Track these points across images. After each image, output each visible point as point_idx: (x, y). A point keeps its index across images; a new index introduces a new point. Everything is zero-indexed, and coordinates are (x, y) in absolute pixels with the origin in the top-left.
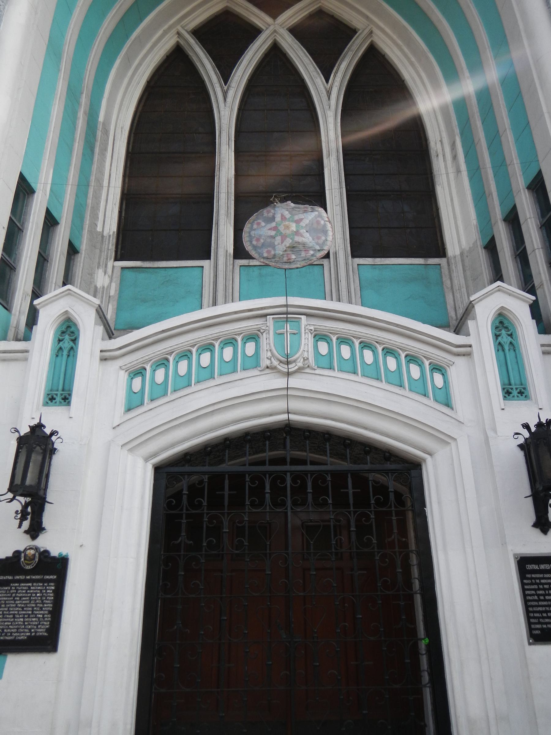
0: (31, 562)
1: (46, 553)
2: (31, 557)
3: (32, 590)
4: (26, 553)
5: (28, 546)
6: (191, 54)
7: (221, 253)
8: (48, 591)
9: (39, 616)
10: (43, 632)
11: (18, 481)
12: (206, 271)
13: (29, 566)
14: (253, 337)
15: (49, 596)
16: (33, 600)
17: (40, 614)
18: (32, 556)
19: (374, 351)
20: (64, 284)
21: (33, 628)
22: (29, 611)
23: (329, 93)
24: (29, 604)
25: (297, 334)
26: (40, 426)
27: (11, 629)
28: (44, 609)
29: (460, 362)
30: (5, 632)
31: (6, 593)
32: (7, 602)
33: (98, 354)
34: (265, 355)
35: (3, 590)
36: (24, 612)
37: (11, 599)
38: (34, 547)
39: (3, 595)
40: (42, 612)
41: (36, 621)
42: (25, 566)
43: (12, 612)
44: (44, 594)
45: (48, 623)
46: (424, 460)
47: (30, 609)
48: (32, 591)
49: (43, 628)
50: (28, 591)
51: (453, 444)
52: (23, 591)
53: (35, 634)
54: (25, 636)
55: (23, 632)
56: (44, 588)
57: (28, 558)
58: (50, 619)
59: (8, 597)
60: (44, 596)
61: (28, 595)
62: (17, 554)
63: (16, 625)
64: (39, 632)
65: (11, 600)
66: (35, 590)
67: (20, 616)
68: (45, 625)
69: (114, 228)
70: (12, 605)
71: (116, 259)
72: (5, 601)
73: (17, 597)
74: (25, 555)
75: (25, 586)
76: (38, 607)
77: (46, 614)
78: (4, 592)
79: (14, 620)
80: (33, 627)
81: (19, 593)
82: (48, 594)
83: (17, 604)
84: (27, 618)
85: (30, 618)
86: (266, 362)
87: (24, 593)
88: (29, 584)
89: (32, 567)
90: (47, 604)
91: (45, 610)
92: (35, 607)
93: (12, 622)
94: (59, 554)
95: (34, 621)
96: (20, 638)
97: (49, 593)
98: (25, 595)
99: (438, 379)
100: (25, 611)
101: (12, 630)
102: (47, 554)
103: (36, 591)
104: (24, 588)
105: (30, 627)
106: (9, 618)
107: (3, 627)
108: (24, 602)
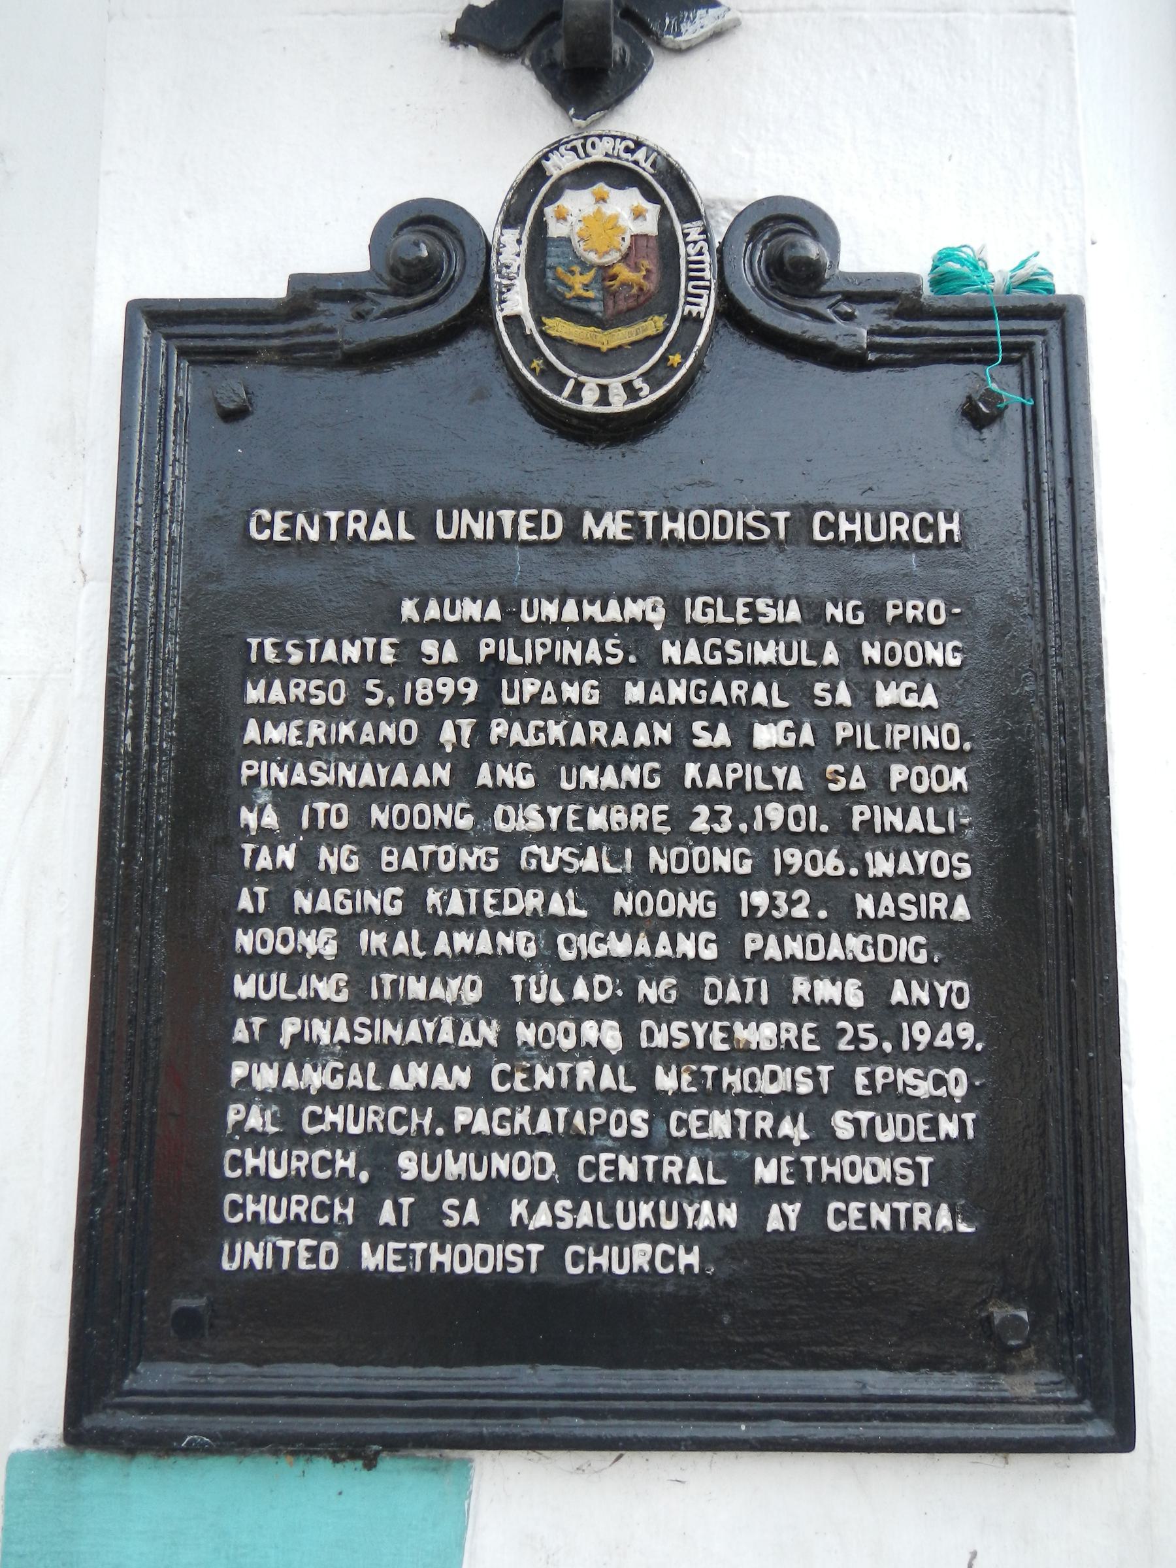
0: (622, 336)
2: (626, 273)
3: (692, 670)
4: (540, 225)
5: (555, 147)
8: (886, 696)
9: (826, 991)
10: (903, 1193)
13: (616, 385)
15: (912, 753)
16: (712, 796)
17: (840, 970)
18: (625, 258)
21: (775, 1145)
22: (690, 924)
24: (664, 842)
27: (484, 1145)
28: (865, 904)
30: (416, 1186)
31: (356, 708)
32: (379, 816)
35: (306, 670)
36: (620, 947)
37: (421, 778)
38: (646, 170)
39: (316, 729)
40: (854, 943)
41: (787, 1055)
42: (550, 374)
43: (463, 941)
44: (843, 730)
45: (958, 1083)
47: (694, 904)
48: (677, 693)
49: (896, 1148)
50: (634, 693)
52: (570, 692)
53: (813, 1214)
54: (685, 1235)
55: (643, 1189)
56: (831, 656)
57: (578, 282)
58: (967, 1031)
59: (384, 752)
60: (850, 750)
61: (642, 737)
63: (541, 1098)
64: (848, 1191)
65: (433, 794)
66: (726, 672)
67: (580, 991)
68: (911, 1104)
70: (448, 857)
72: (359, 799)
73: (511, 753)
74: (539, 242)
75: (583, 630)
76: (791, 880)
77: (907, 970)
78: (335, 694)
79: (507, 1036)
80: (764, 1122)
81: (519, 714)
82: (897, 734)
83: (511, 843)
84: (662, 1013)
85: (706, 1014)
87: (584, 713)
88: (634, 610)
89: (648, 397)
90: (893, 841)
91: (896, 925)
92: (750, 882)
93: (476, 1059)
94: (944, 256)
95: (758, 1057)
96: (603, 1259)
97: (897, 712)
98: (598, 730)
100: (629, 924)
101: (500, 1164)
102: (813, 250)
103: (738, 689)
104: (570, 651)
105: (720, 1125)
106: (432, 1008)
107: (373, 1115)
108: (596, 820)
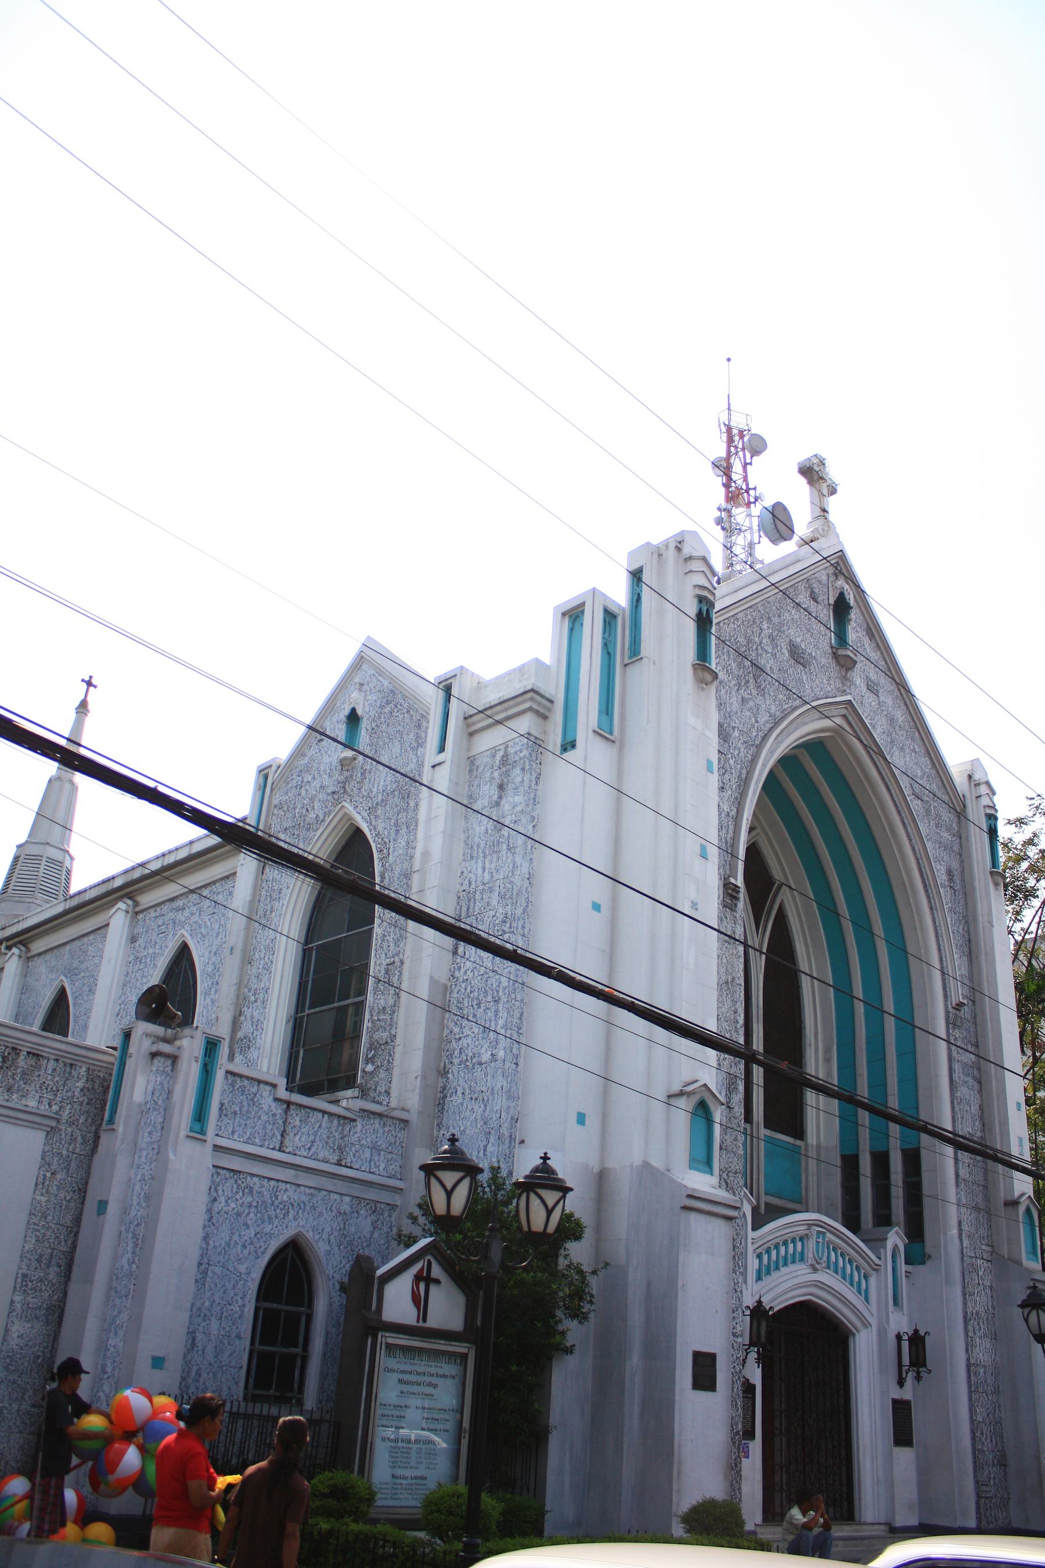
1: (748, 1380)
26: (759, 1302)
34: (810, 1255)
46: (854, 1335)
51: (869, 1329)
86: (810, 1262)
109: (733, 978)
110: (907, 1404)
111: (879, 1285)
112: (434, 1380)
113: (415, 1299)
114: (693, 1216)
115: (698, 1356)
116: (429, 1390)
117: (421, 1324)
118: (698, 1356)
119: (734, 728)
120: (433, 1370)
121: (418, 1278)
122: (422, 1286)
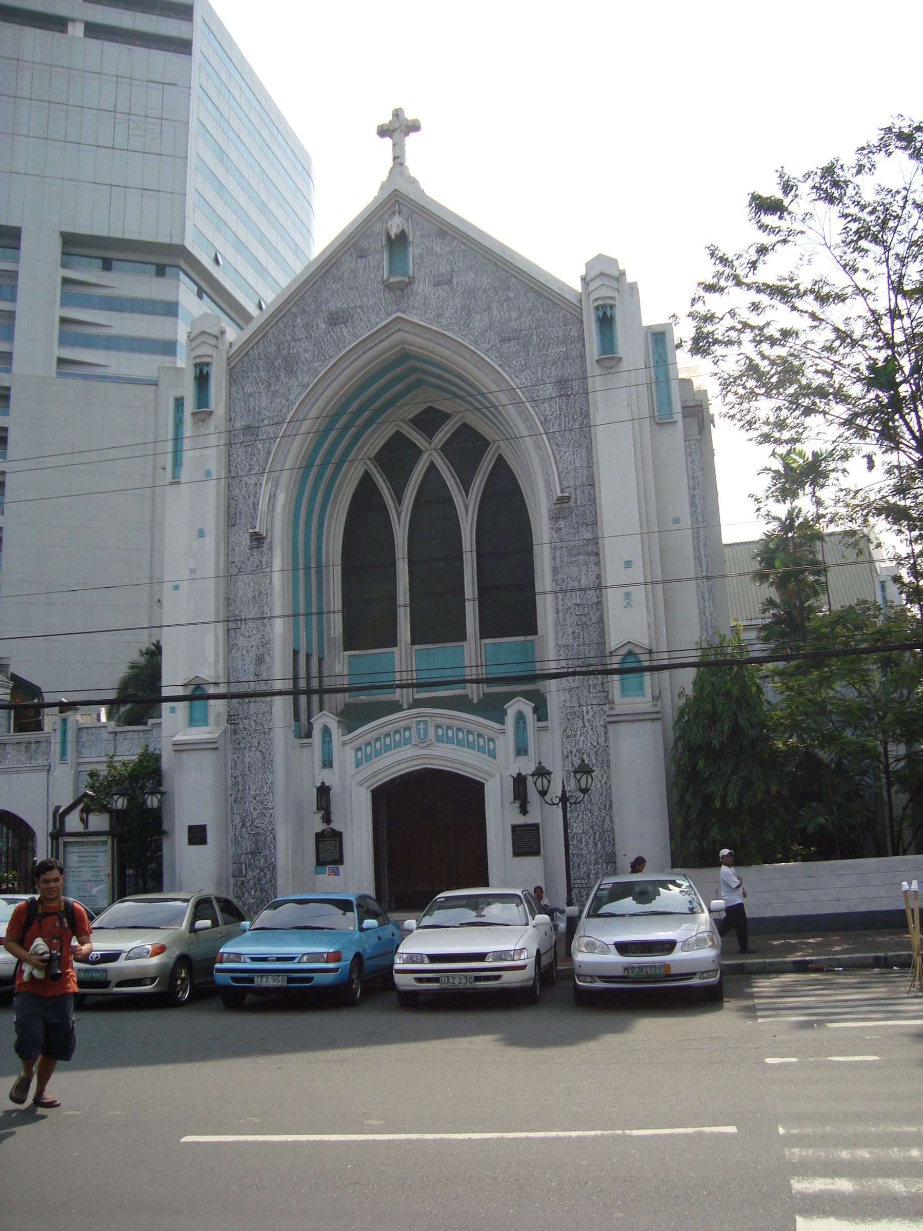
1: (333, 830)
6: (373, 477)
7: (403, 644)
11: (319, 806)
12: (397, 656)
14: (408, 728)
19: (463, 733)
20: (321, 712)
23: (466, 507)
25: (426, 729)
26: (323, 783)
29: (501, 736)
33: (341, 743)
34: (413, 739)
62: (323, 831)
69: (341, 630)
71: (345, 650)
86: (414, 742)
99: (491, 744)
109: (260, 592)
110: (536, 826)
111: (506, 742)
112: (96, 854)
113: (82, 820)
114: (184, 754)
115: (191, 828)
116: (94, 859)
117: (86, 830)
118: (191, 828)
119: (263, 421)
120: (95, 850)
121: (82, 811)
122: (85, 815)
